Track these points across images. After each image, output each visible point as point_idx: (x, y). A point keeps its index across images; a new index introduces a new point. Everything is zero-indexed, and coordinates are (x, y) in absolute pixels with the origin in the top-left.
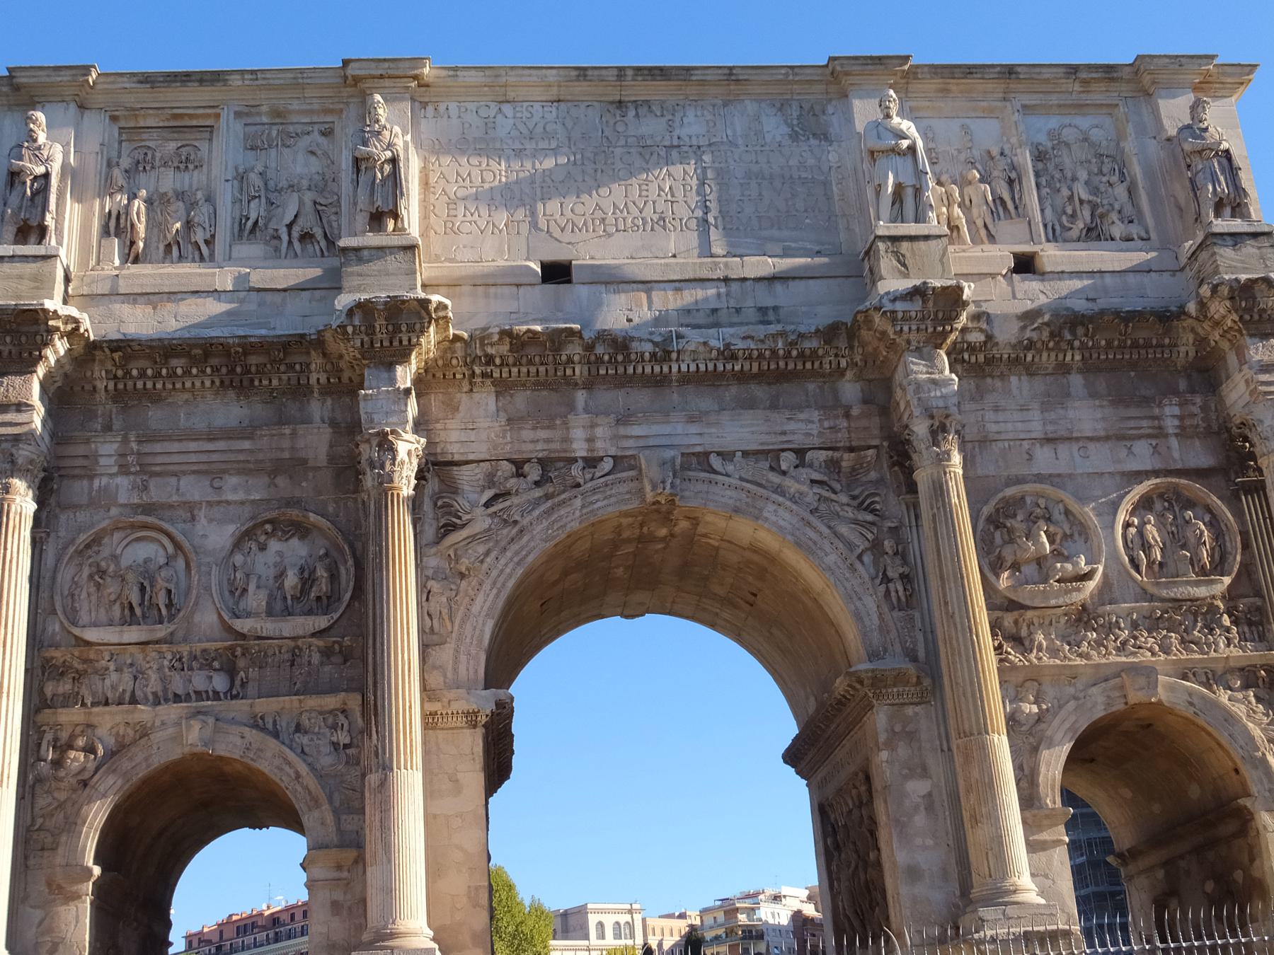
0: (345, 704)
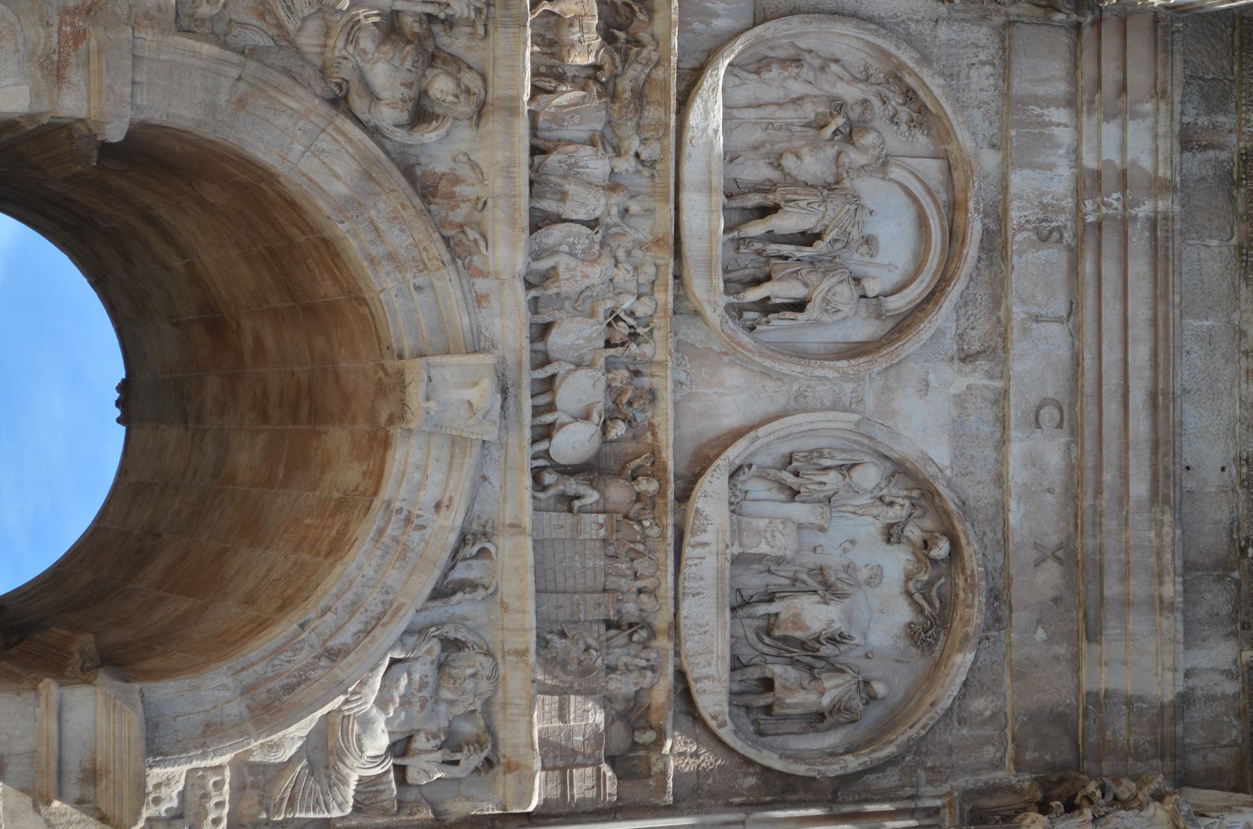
0: (509, 768)
